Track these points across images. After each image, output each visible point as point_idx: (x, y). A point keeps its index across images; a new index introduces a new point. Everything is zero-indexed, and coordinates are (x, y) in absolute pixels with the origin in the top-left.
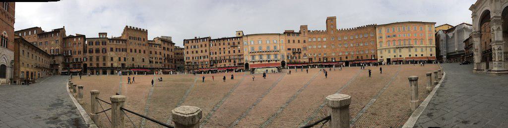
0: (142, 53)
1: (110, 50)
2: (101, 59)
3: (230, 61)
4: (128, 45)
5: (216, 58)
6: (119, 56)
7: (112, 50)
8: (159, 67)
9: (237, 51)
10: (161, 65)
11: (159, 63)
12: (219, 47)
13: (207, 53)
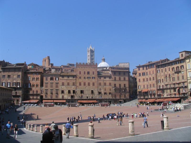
0: (91, 85)
1: (61, 84)
2: (54, 92)
3: (174, 89)
4: (77, 79)
5: (163, 86)
6: (69, 89)
7: (63, 84)
8: (107, 98)
9: (181, 78)
10: (110, 95)
11: (108, 94)
12: (166, 73)
13: (154, 82)
